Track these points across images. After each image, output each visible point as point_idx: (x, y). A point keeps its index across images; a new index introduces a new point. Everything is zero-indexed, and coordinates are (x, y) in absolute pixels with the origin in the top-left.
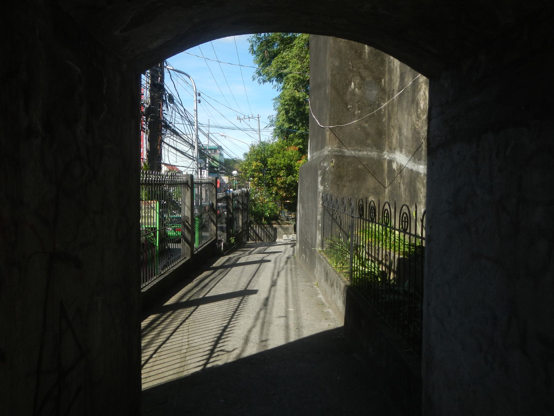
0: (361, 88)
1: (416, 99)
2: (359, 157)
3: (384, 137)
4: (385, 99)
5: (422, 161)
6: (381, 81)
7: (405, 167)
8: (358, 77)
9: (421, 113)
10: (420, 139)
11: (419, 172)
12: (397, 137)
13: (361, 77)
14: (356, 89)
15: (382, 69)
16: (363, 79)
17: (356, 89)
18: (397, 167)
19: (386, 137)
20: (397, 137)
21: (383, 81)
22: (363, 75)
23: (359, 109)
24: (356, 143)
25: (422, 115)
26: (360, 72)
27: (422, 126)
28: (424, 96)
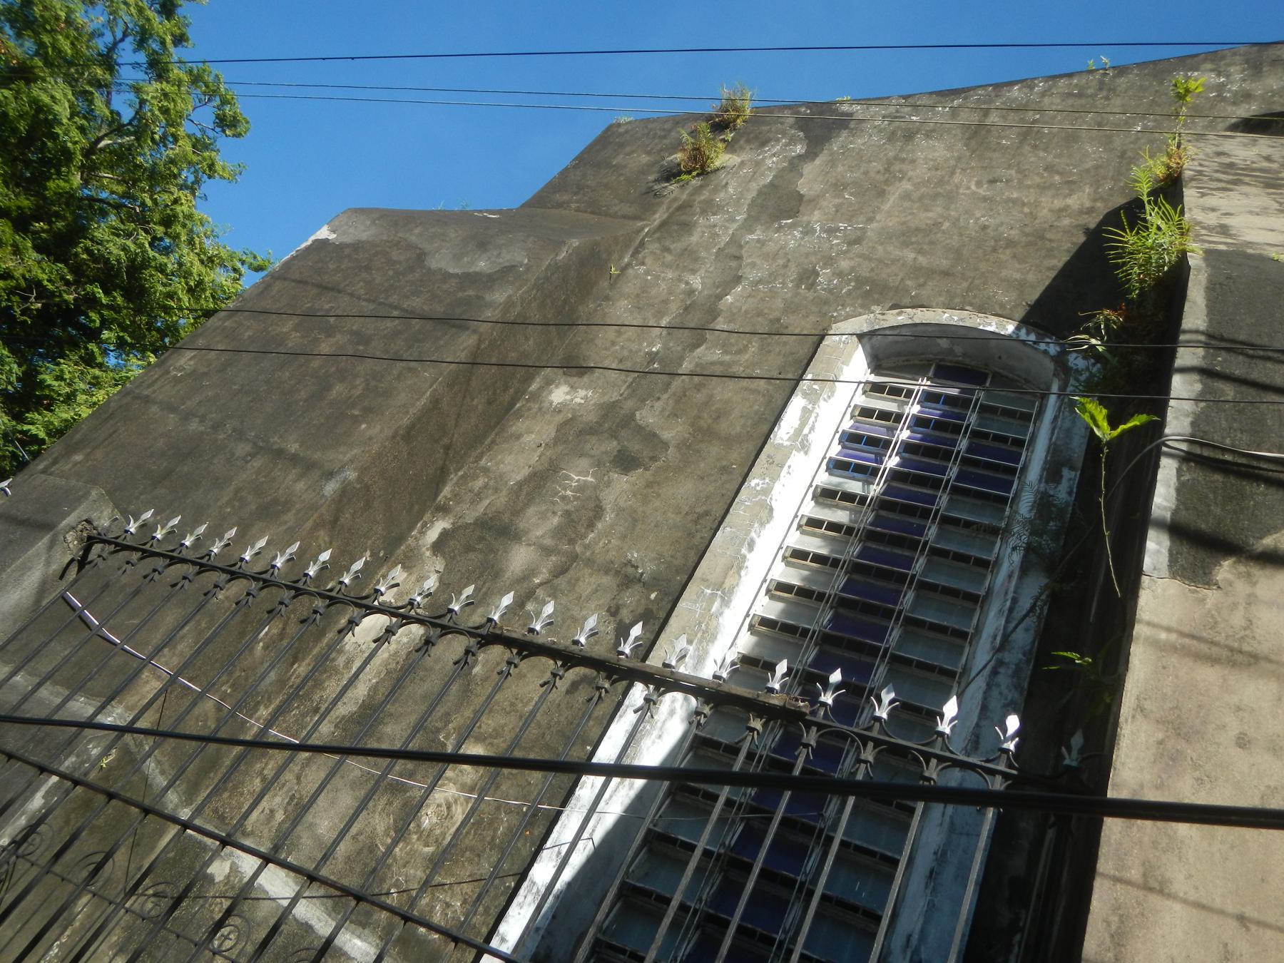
0: (268, 647)
1: (408, 794)
2: (151, 785)
3: (212, 775)
4: (271, 703)
5: (366, 931)
6: (293, 664)
7: (274, 899)
8: (281, 626)
9: (416, 833)
10: (383, 880)
11: (341, 949)
12: (272, 811)
13: (284, 629)
14: (261, 644)
15: (311, 644)
16: (282, 635)
17: (261, 644)
18: (228, 877)
19: (213, 779)
20: (272, 811)
21: (295, 666)
22: (288, 630)
23: (232, 686)
24: (174, 748)
25: (418, 839)
26: (289, 618)
27: (408, 862)
28: (444, 808)
